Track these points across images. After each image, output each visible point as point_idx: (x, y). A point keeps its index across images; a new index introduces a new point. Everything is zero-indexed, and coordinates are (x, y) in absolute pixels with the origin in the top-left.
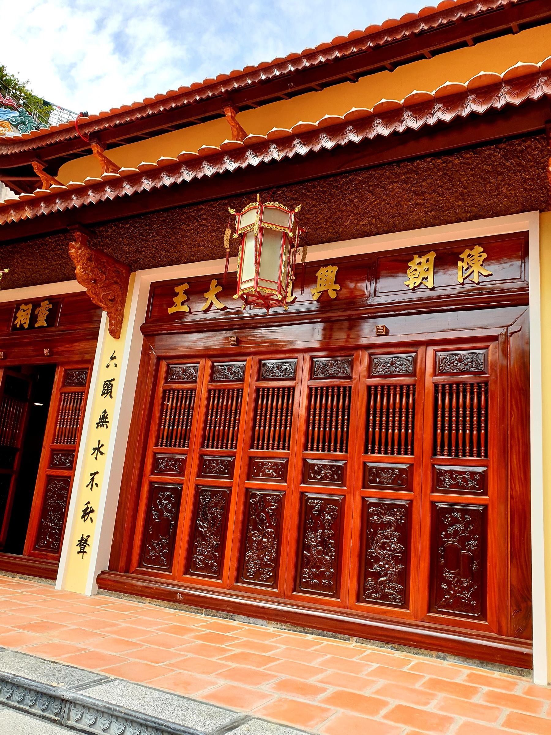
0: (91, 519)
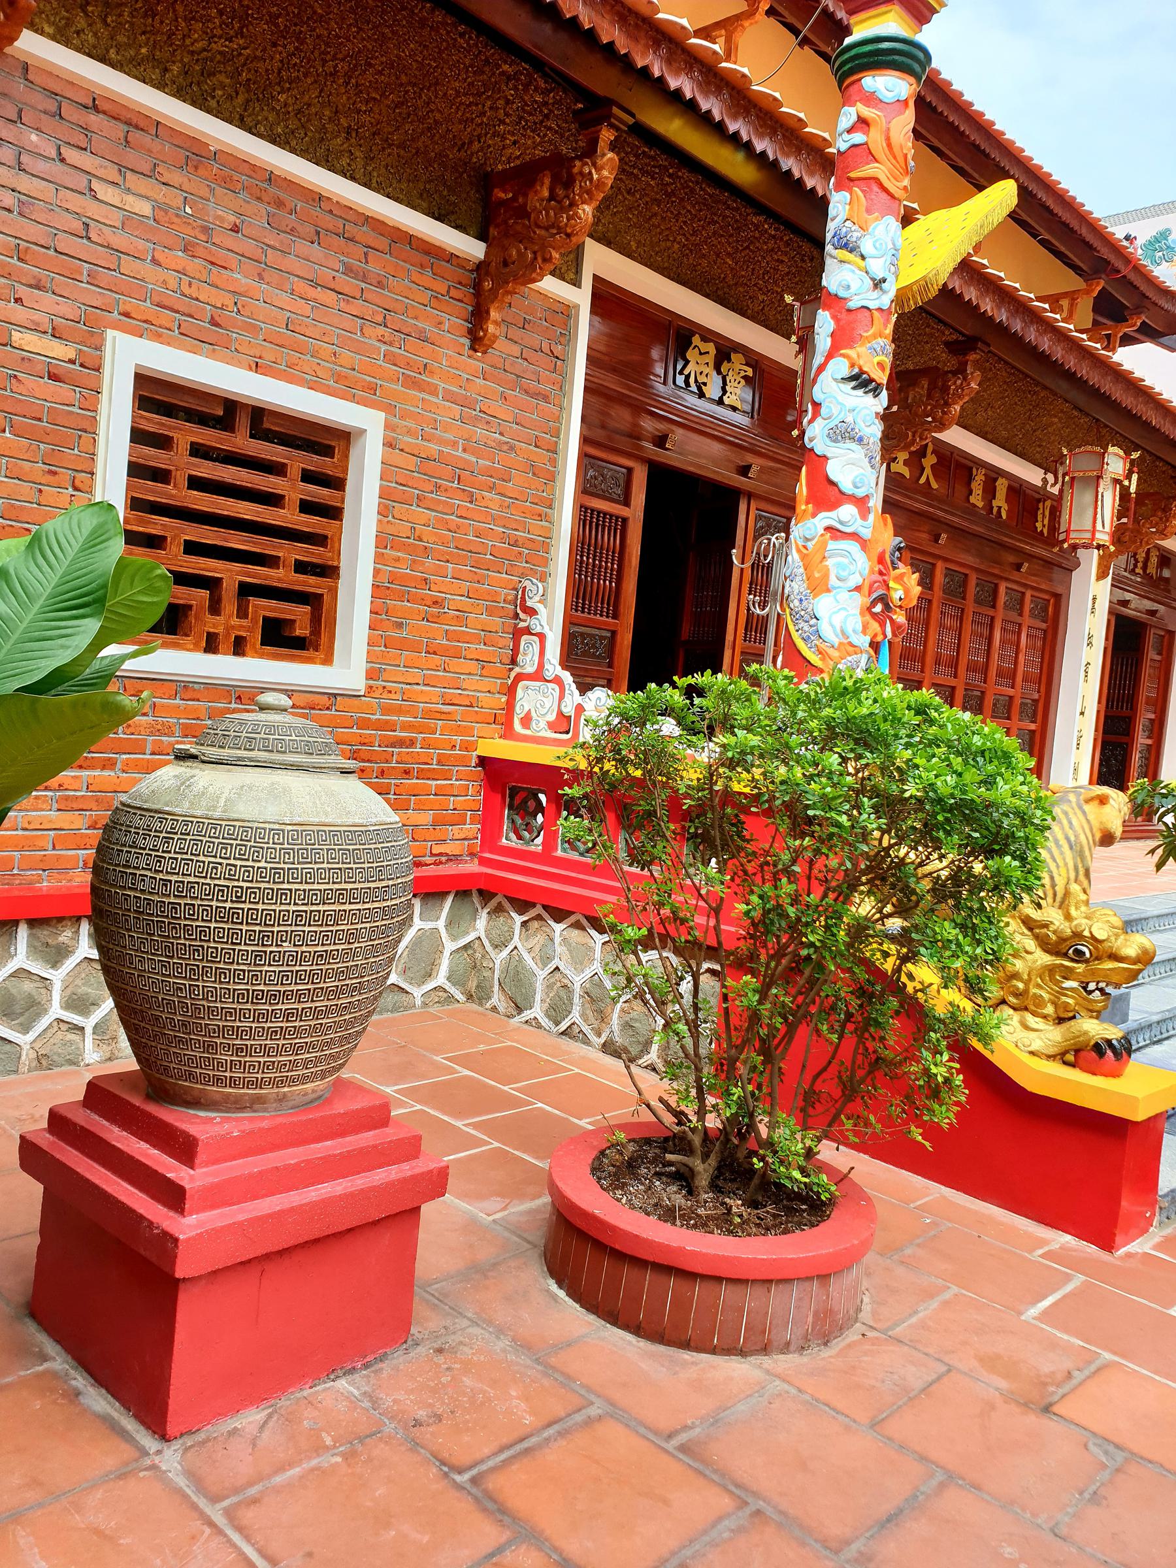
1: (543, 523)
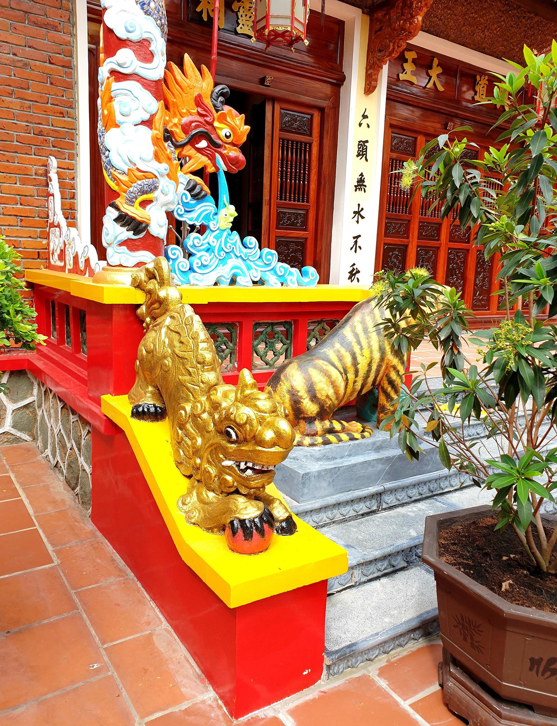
0: (358, 279)
1: (66, 119)
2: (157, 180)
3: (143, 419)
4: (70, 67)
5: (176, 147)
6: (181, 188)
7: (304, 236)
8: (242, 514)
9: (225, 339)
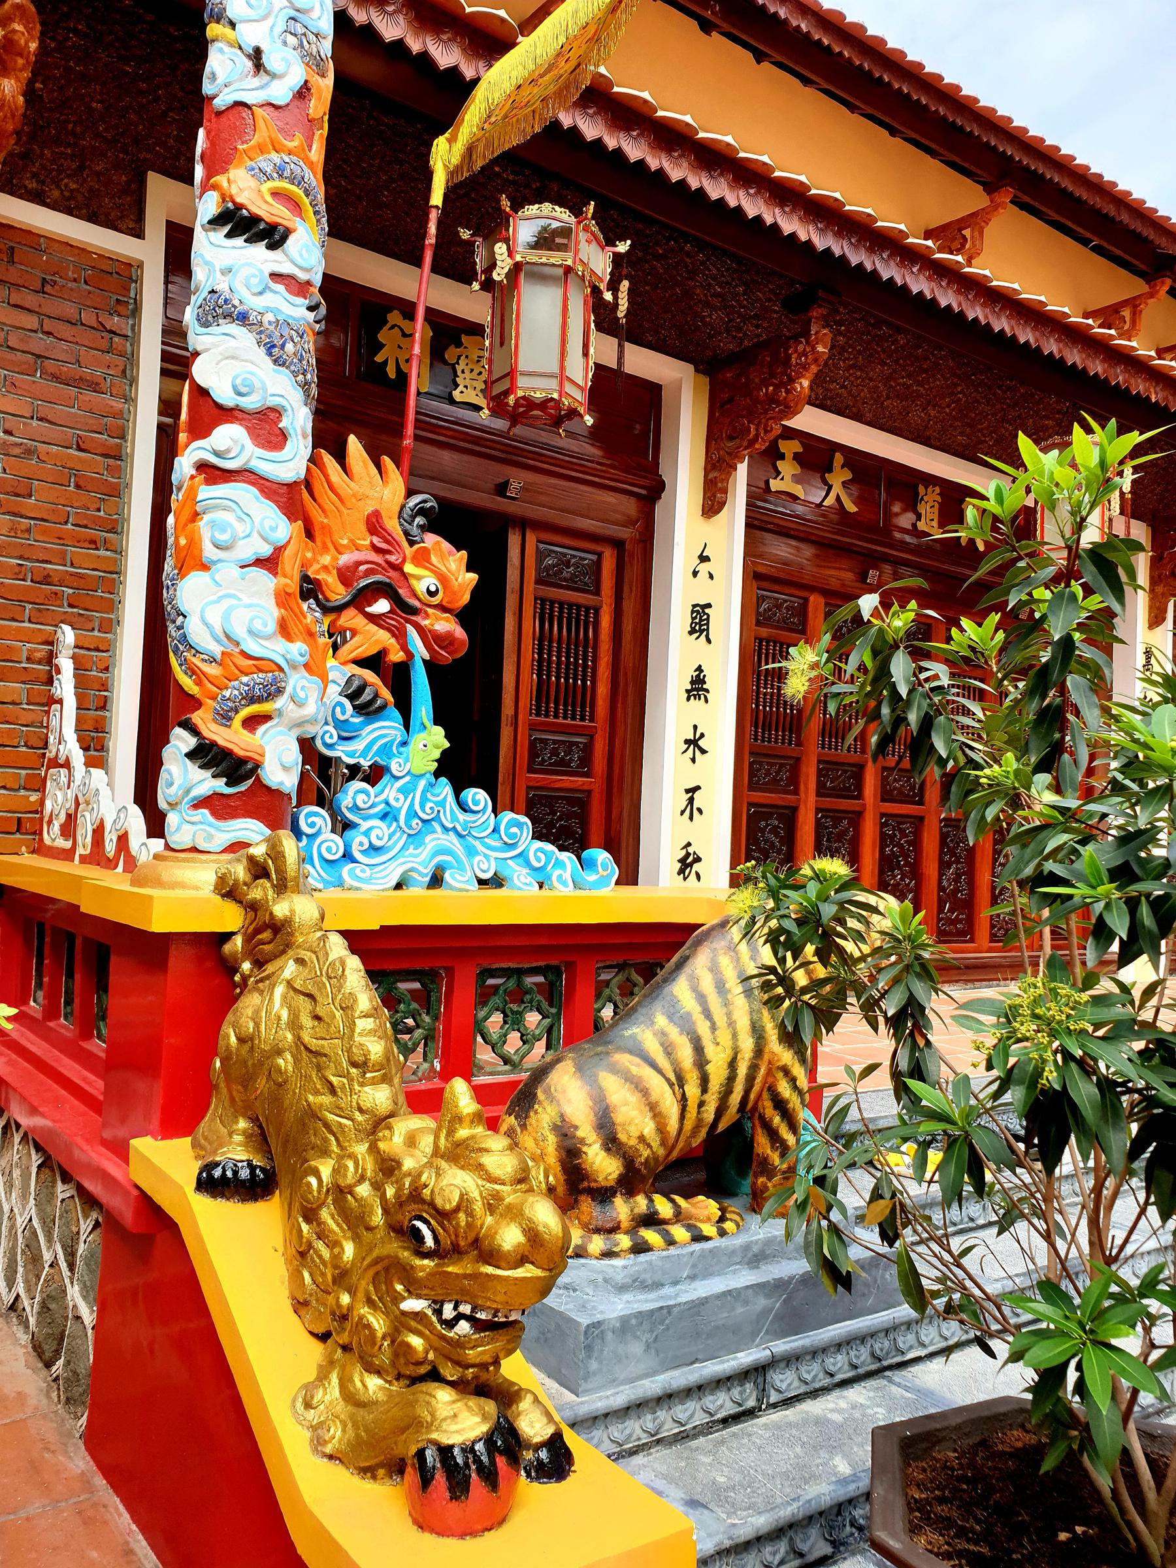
1: (102, 552)
2: (282, 675)
3: (223, 1196)
4: (118, 457)
5: (326, 610)
6: (334, 691)
7: (585, 787)
8: (445, 1431)
9: (414, 1005)
